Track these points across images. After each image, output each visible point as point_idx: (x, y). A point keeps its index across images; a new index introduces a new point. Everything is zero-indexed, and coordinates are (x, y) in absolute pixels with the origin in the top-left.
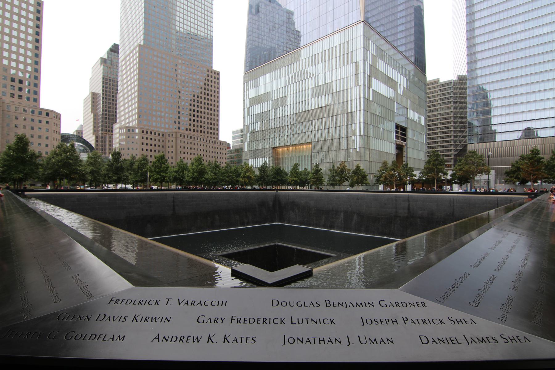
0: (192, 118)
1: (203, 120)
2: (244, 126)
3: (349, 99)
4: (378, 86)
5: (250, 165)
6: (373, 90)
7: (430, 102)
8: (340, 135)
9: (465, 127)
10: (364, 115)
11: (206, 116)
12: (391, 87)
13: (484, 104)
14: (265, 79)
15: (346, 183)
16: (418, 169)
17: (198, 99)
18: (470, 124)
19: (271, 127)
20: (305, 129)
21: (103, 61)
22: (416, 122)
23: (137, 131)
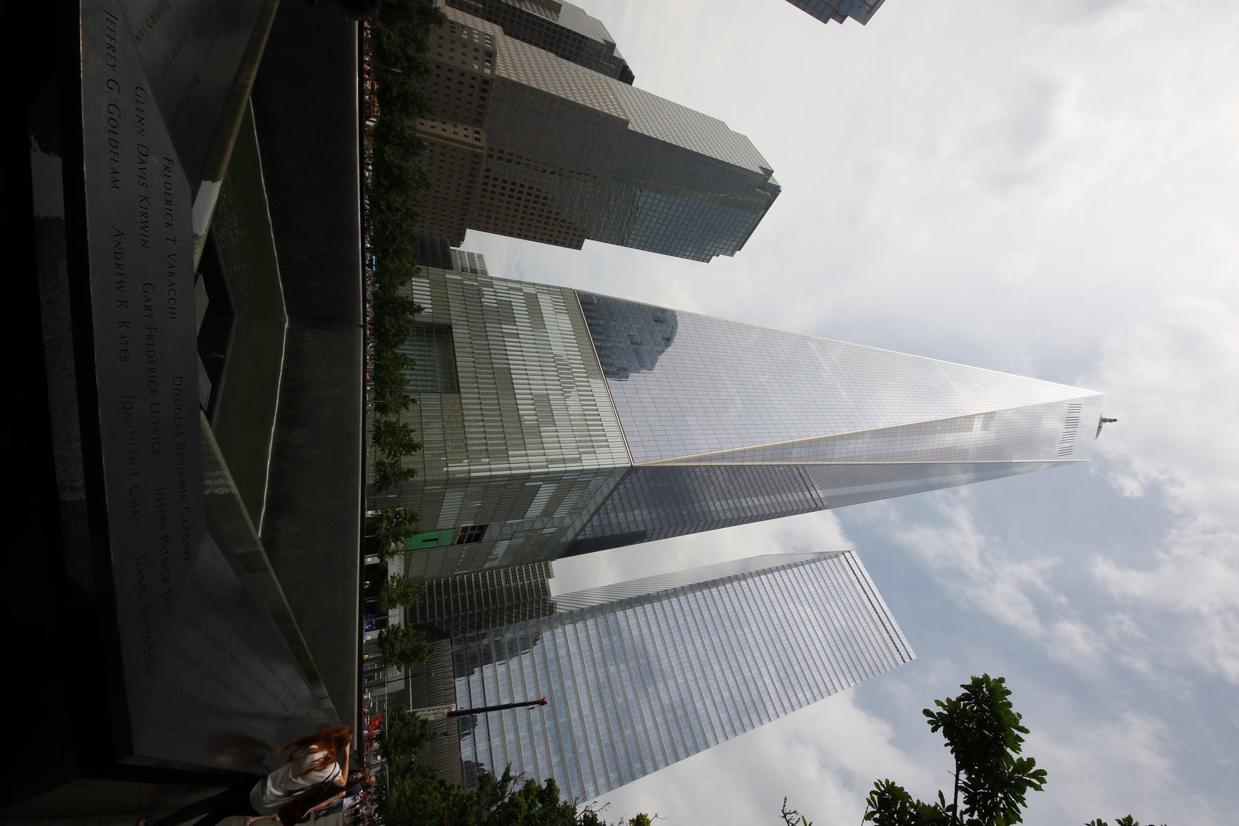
0: (508, 187)
4: (545, 493)
6: (540, 486)
9: (479, 628)
14: (565, 322)
21: (611, 46)
22: (490, 554)
23: (488, 71)
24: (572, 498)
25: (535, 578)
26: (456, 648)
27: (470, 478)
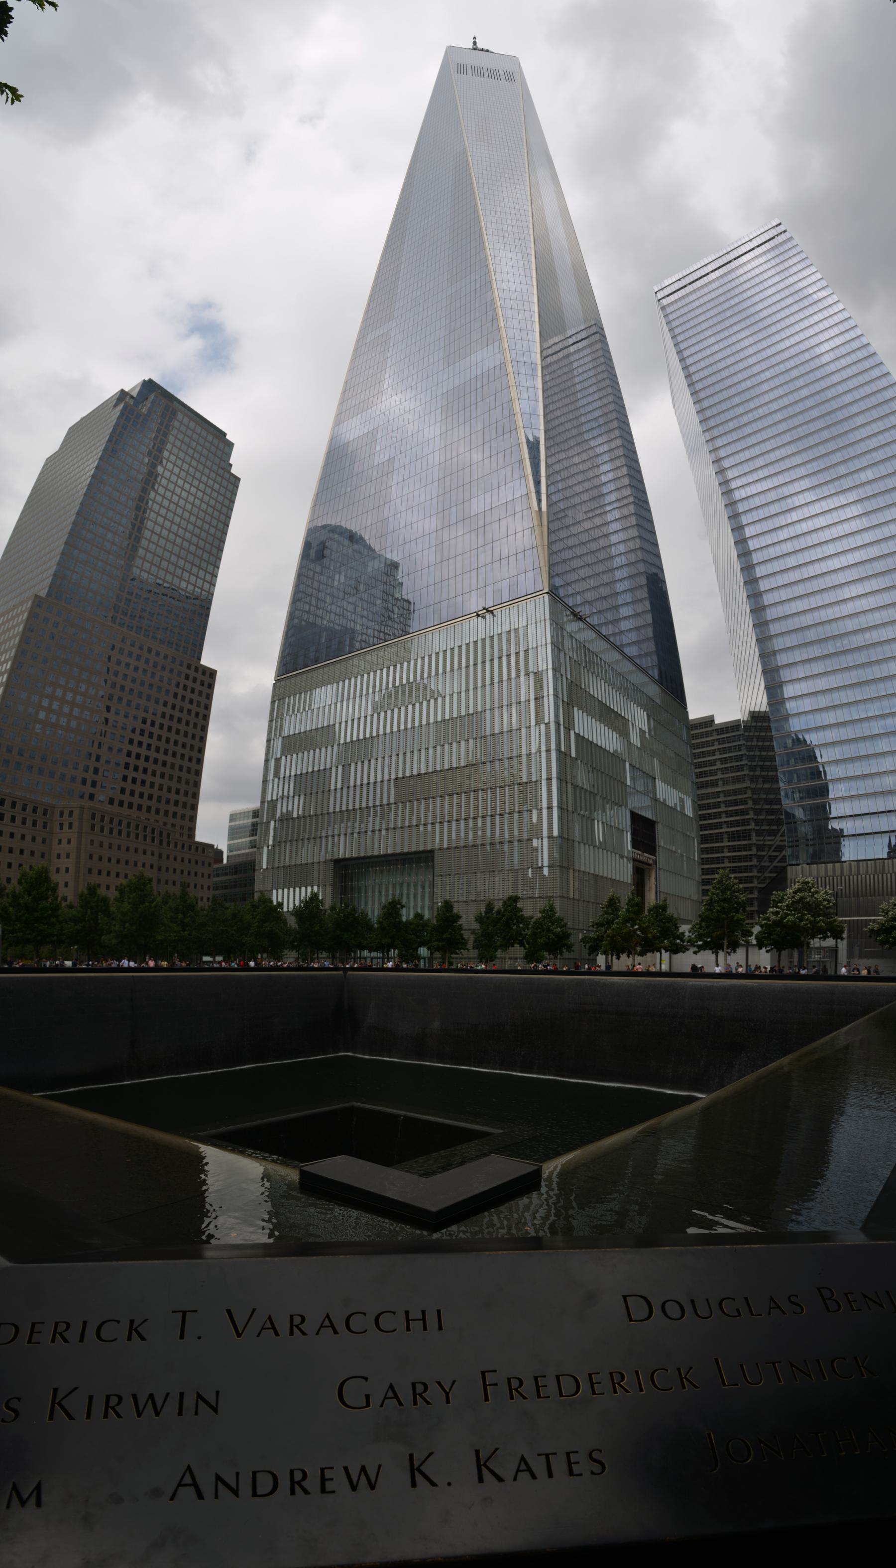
1: (157, 780)
2: (263, 802)
3: (524, 752)
4: (587, 726)
5: (275, 903)
6: (577, 735)
7: (699, 765)
8: (502, 834)
9: (779, 822)
10: (560, 789)
11: (167, 770)
12: (614, 729)
13: (812, 774)
14: (324, 695)
16: (686, 922)
17: (153, 730)
18: (790, 816)
19: (331, 810)
20: (419, 819)
22: (674, 809)
24: (599, 689)
25: (711, 744)
26: (803, 856)
27: (561, 836)
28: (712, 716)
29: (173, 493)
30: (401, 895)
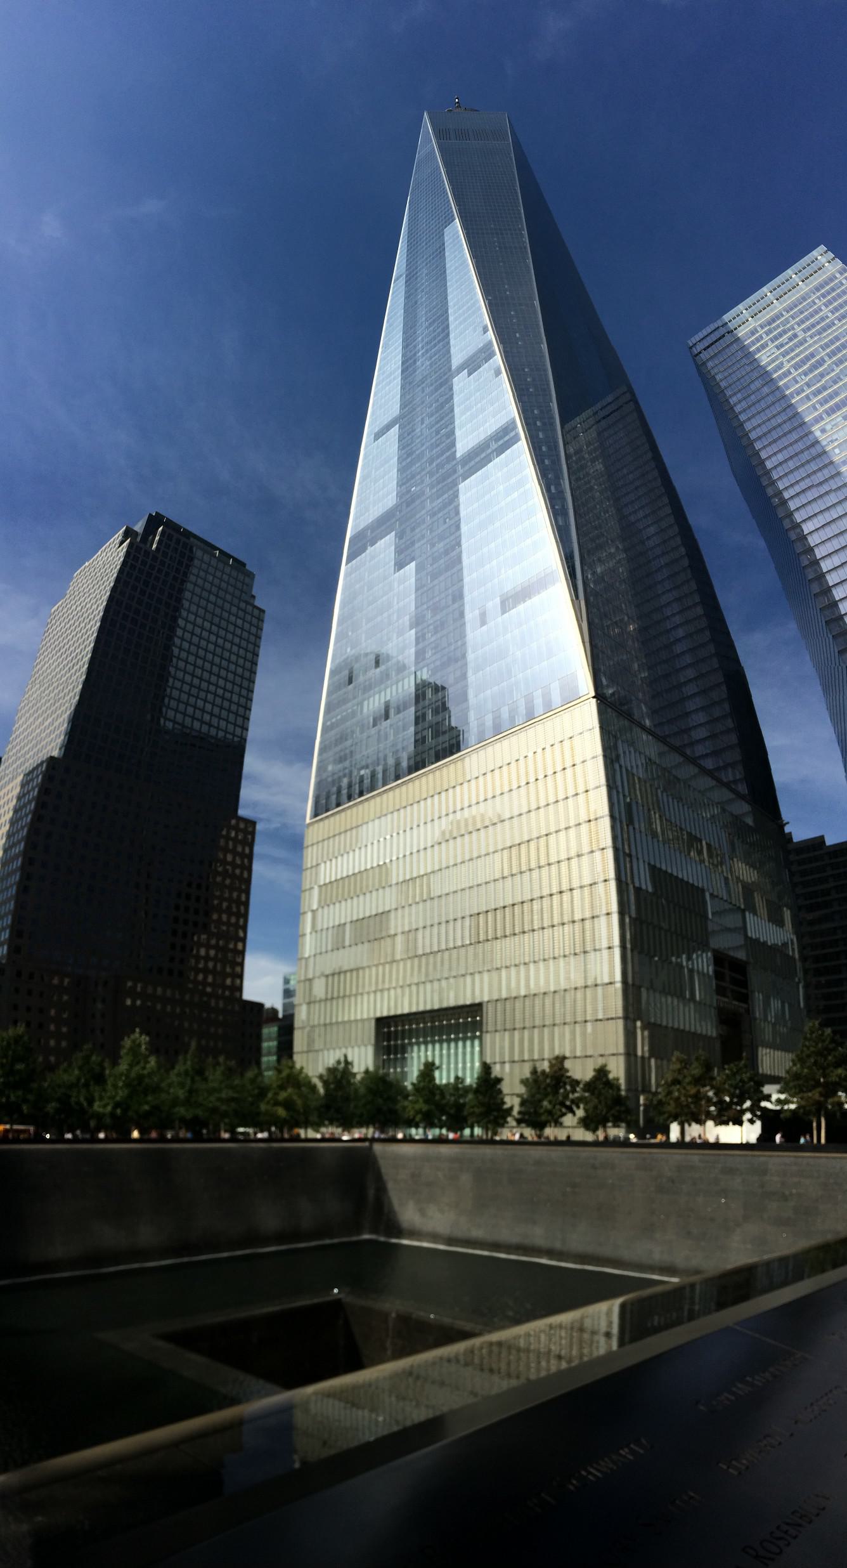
15: (568, 1120)
28: (822, 837)
29: (193, 634)
30: (434, 1056)
